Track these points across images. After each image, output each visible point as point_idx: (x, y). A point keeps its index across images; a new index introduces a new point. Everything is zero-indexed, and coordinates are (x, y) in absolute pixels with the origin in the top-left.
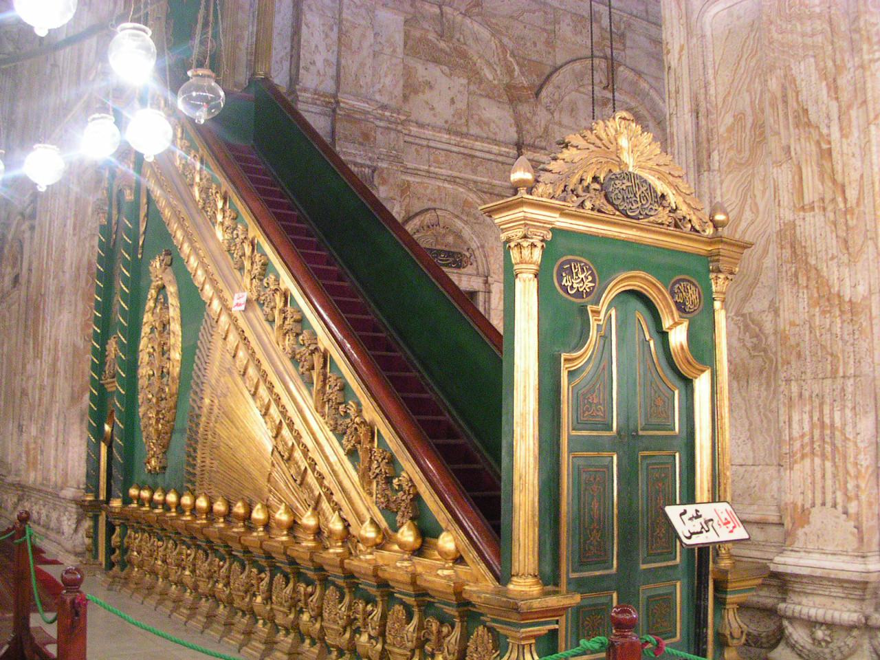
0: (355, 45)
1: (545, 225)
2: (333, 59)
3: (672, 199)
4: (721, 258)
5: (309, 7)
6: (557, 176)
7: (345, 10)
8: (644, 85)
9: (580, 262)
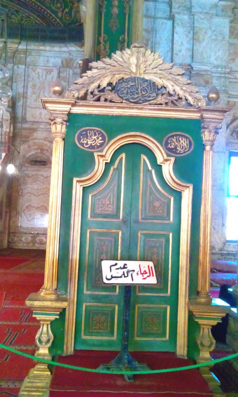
1: (63, 112)
2: (190, 47)
3: (170, 89)
4: (205, 120)
5: (178, 24)
6: (81, 86)
7: (195, 22)
9: (94, 130)
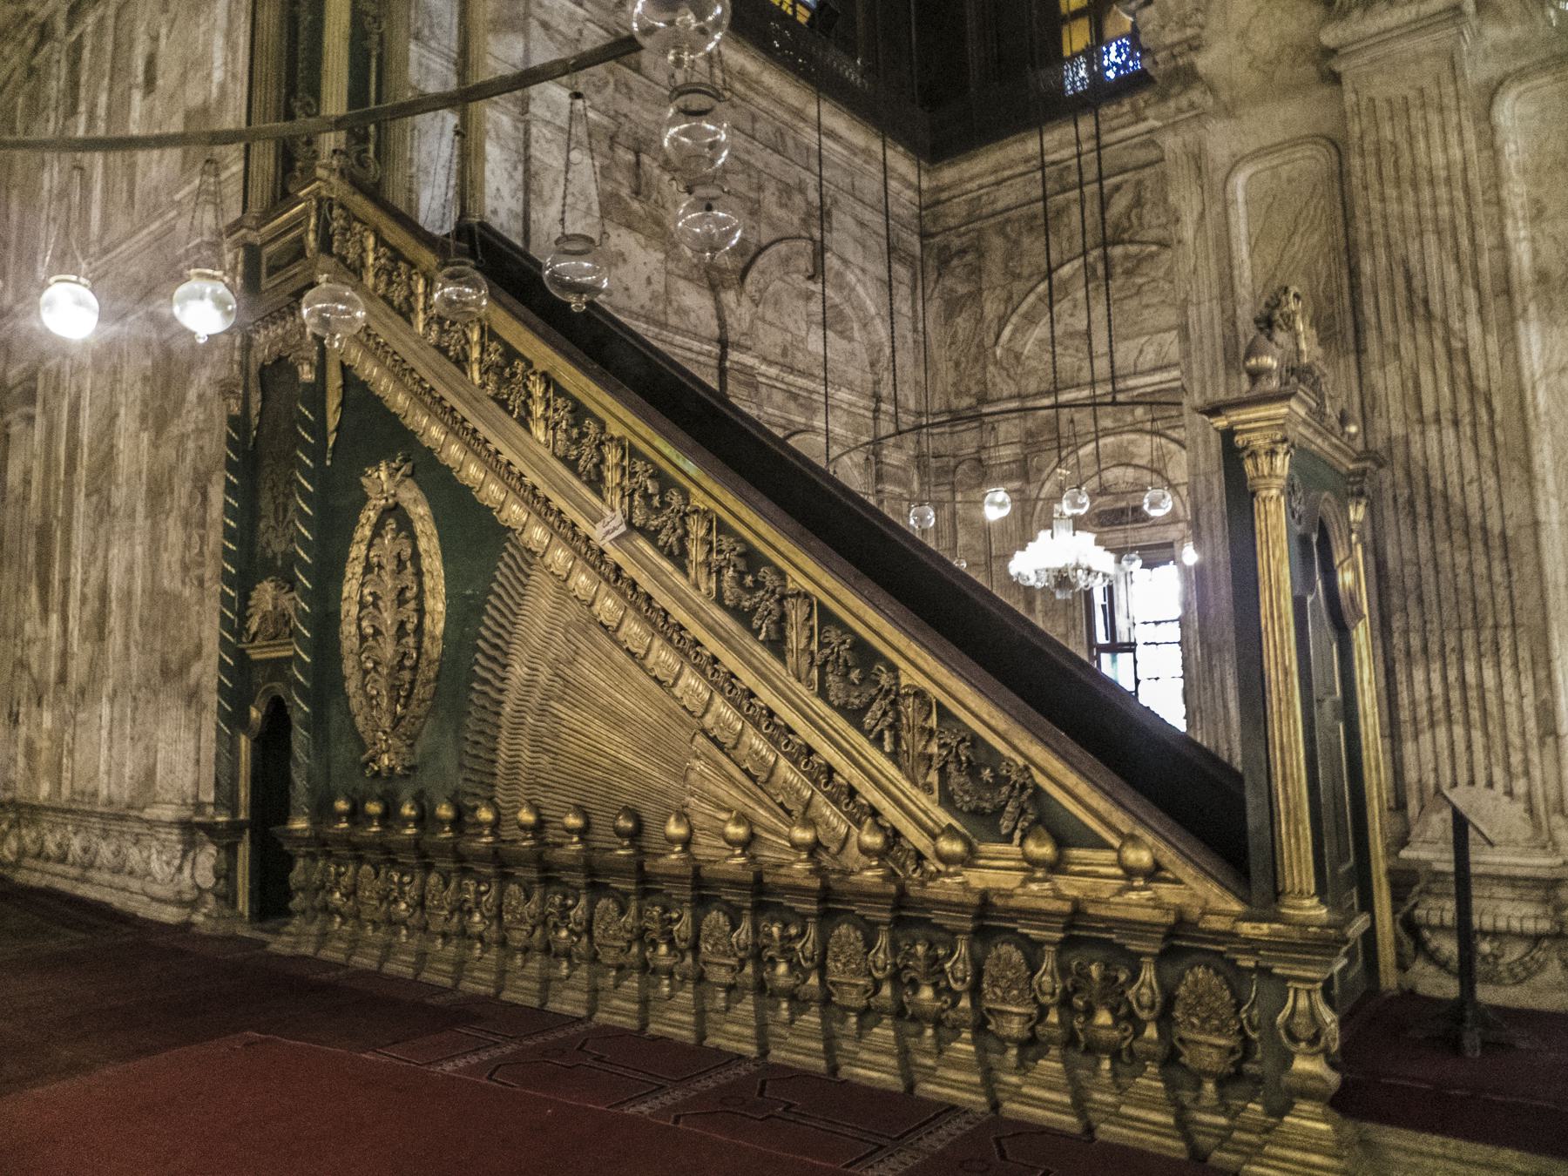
0: (547, 193)
2: (518, 208)
8: (851, 278)
